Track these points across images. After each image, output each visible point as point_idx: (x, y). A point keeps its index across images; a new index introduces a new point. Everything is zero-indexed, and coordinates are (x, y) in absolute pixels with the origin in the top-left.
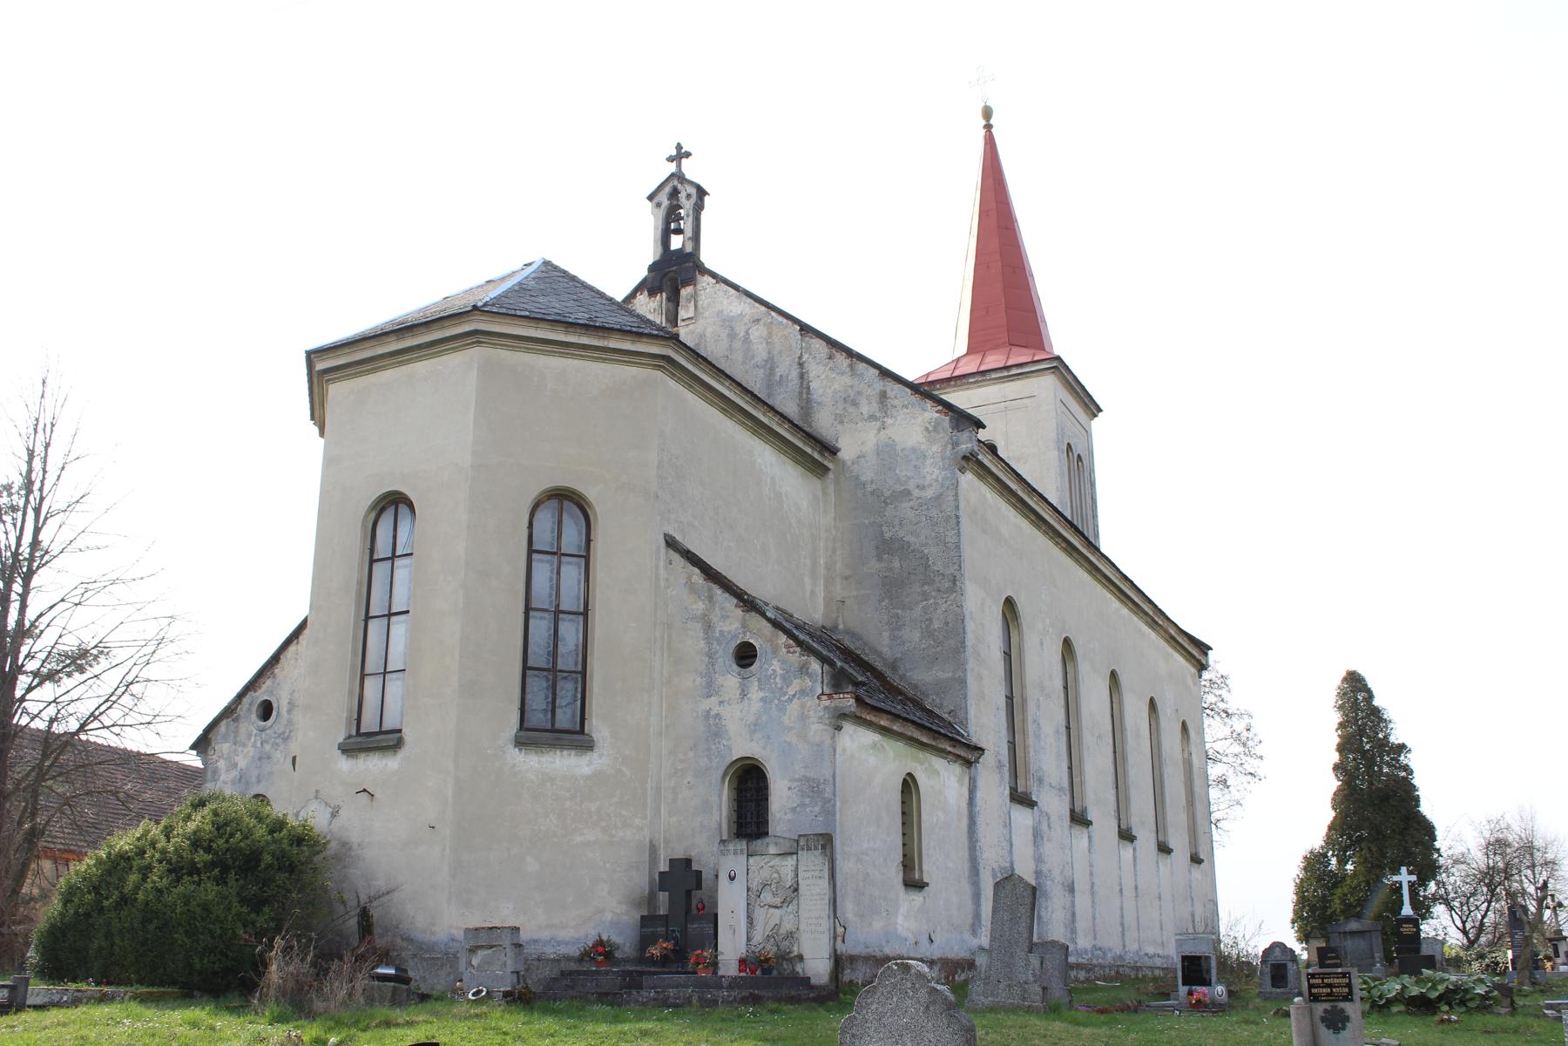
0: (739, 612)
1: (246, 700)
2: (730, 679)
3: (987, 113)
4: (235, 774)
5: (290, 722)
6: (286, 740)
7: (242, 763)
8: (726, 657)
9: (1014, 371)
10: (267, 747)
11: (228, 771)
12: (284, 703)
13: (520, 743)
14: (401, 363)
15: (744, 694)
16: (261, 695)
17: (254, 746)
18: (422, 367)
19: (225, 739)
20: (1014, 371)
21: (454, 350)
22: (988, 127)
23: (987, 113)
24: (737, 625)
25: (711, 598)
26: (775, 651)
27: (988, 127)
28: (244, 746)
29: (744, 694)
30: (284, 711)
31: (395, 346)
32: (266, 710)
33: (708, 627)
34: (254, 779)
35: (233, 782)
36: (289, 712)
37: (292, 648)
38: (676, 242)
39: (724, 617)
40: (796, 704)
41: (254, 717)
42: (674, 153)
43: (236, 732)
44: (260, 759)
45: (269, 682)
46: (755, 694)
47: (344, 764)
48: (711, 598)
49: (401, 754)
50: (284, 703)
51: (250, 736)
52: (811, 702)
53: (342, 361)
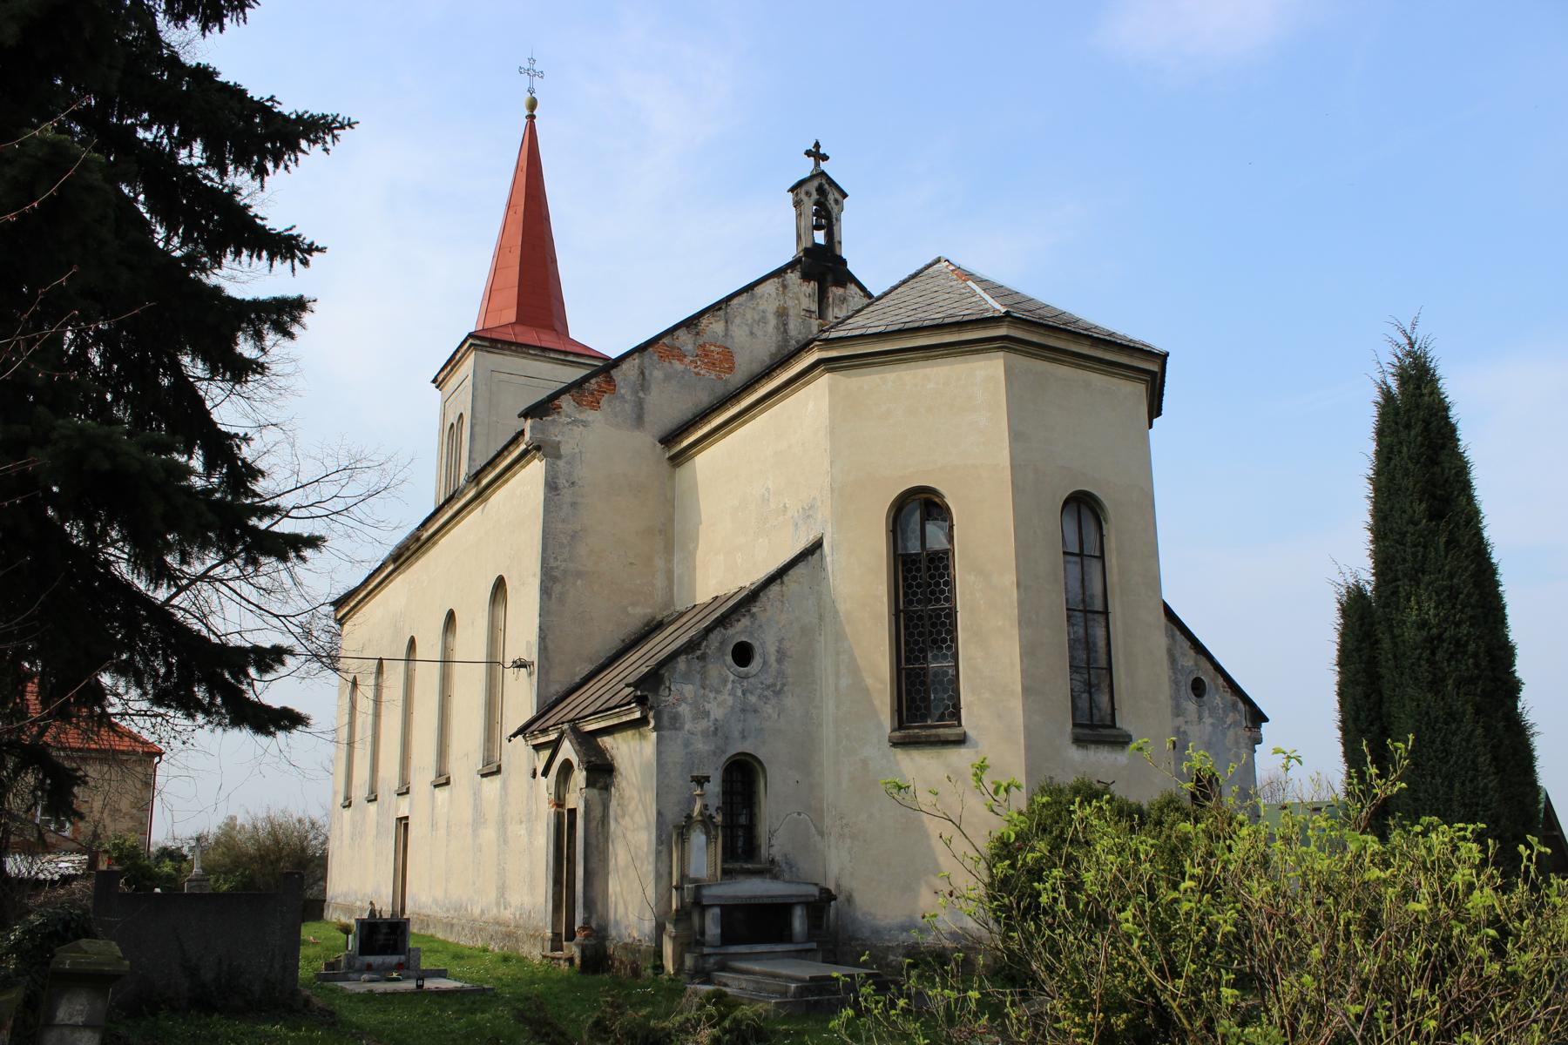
0: (1192, 652)
1: (715, 637)
2: (1191, 706)
3: (532, 105)
4: (704, 724)
5: (781, 674)
6: (778, 693)
7: (717, 712)
8: (1186, 689)
9: (570, 358)
10: (753, 699)
11: (694, 719)
12: (772, 649)
13: (1079, 741)
14: (1079, 366)
15: (1200, 718)
16: (739, 631)
17: (732, 693)
18: (1097, 380)
19: (687, 678)
20: (570, 358)
21: (1127, 378)
22: (531, 117)
23: (532, 105)
24: (1191, 663)
25: (1173, 637)
26: (1217, 688)
27: (531, 117)
28: (718, 692)
29: (1200, 718)
30: (772, 659)
31: (1086, 350)
32: (743, 654)
34: (736, 734)
35: (705, 733)
36: (779, 661)
37: (775, 589)
38: (820, 237)
39: (1184, 655)
40: (1231, 733)
41: (729, 659)
42: (822, 151)
43: (704, 674)
44: (743, 711)
45: (745, 621)
46: (1208, 720)
47: (1075, 754)
50: (772, 649)
51: (725, 681)
52: (1241, 732)
53: (1035, 338)
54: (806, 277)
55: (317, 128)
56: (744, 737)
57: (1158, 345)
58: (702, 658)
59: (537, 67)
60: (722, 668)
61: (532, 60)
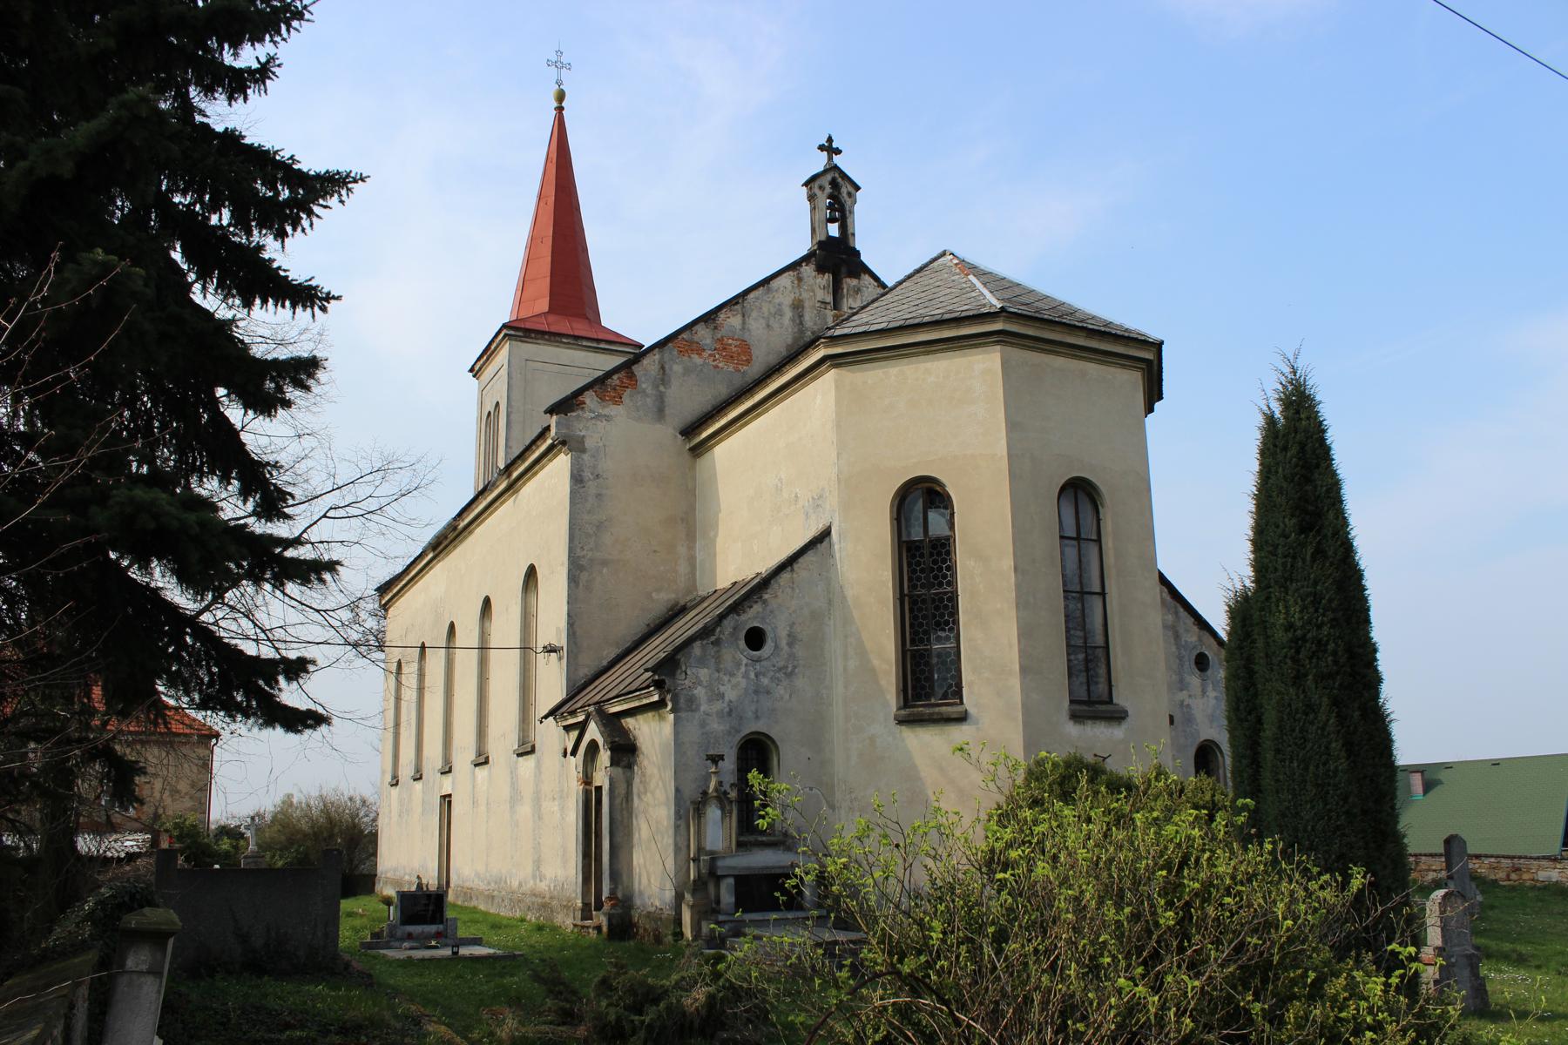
0: (1196, 629)
1: (728, 623)
2: (1194, 680)
3: (561, 96)
4: (719, 706)
5: (792, 656)
6: (789, 675)
7: (731, 694)
9: (602, 346)
10: (765, 681)
11: (710, 701)
12: (783, 633)
15: (1204, 692)
16: (751, 617)
17: (746, 676)
18: (1093, 369)
19: (702, 662)
20: (602, 346)
21: (1123, 366)
22: (560, 109)
23: (561, 96)
25: (1176, 613)
27: (560, 109)
28: (732, 675)
30: (783, 643)
31: (1081, 342)
32: (755, 639)
33: (1177, 636)
34: (750, 714)
35: (720, 714)
36: (790, 644)
37: (785, 576)
38: (834, 230)
39: (1187, 631)
41: (742, 643)
43: (718, 659)
44: (756, 692)
45: (757, 608)
47: (1073, 729)
48: (1176, 613)
49: (1125, 725)
50: (783, 633)
51: (738, 665)
53: (1030, 332)
54: (821, 269)
55: (333, 183)
56: (757, 718)
57: (1154, 333)
58: (717, 643)
59: (565, 60)
60: (736, 652)
61: (559, 53)
